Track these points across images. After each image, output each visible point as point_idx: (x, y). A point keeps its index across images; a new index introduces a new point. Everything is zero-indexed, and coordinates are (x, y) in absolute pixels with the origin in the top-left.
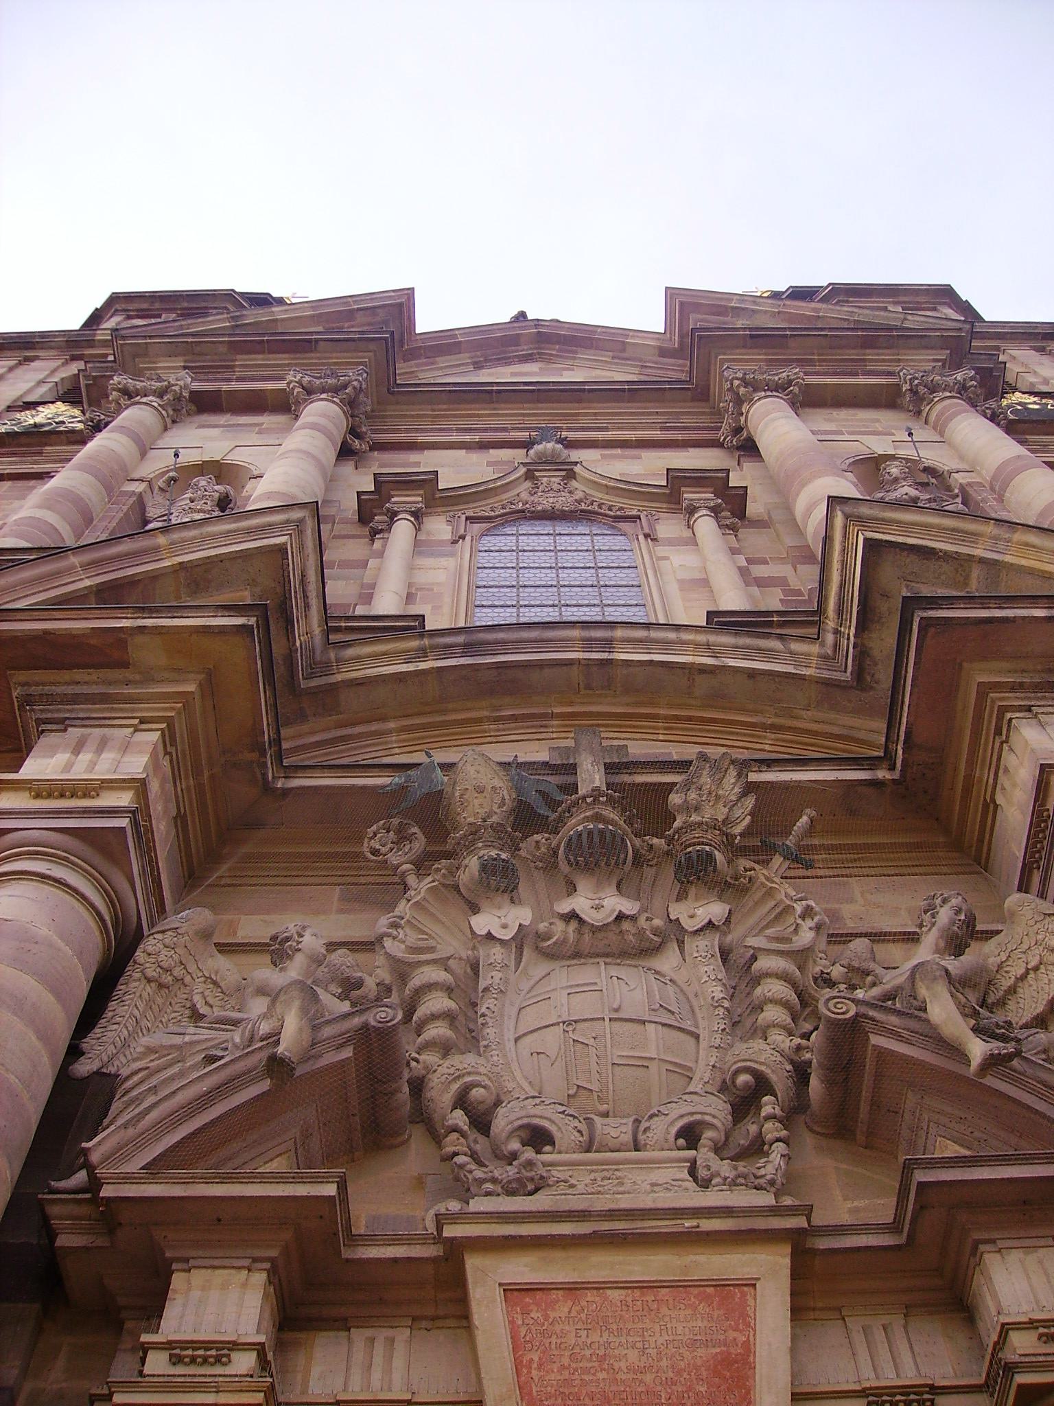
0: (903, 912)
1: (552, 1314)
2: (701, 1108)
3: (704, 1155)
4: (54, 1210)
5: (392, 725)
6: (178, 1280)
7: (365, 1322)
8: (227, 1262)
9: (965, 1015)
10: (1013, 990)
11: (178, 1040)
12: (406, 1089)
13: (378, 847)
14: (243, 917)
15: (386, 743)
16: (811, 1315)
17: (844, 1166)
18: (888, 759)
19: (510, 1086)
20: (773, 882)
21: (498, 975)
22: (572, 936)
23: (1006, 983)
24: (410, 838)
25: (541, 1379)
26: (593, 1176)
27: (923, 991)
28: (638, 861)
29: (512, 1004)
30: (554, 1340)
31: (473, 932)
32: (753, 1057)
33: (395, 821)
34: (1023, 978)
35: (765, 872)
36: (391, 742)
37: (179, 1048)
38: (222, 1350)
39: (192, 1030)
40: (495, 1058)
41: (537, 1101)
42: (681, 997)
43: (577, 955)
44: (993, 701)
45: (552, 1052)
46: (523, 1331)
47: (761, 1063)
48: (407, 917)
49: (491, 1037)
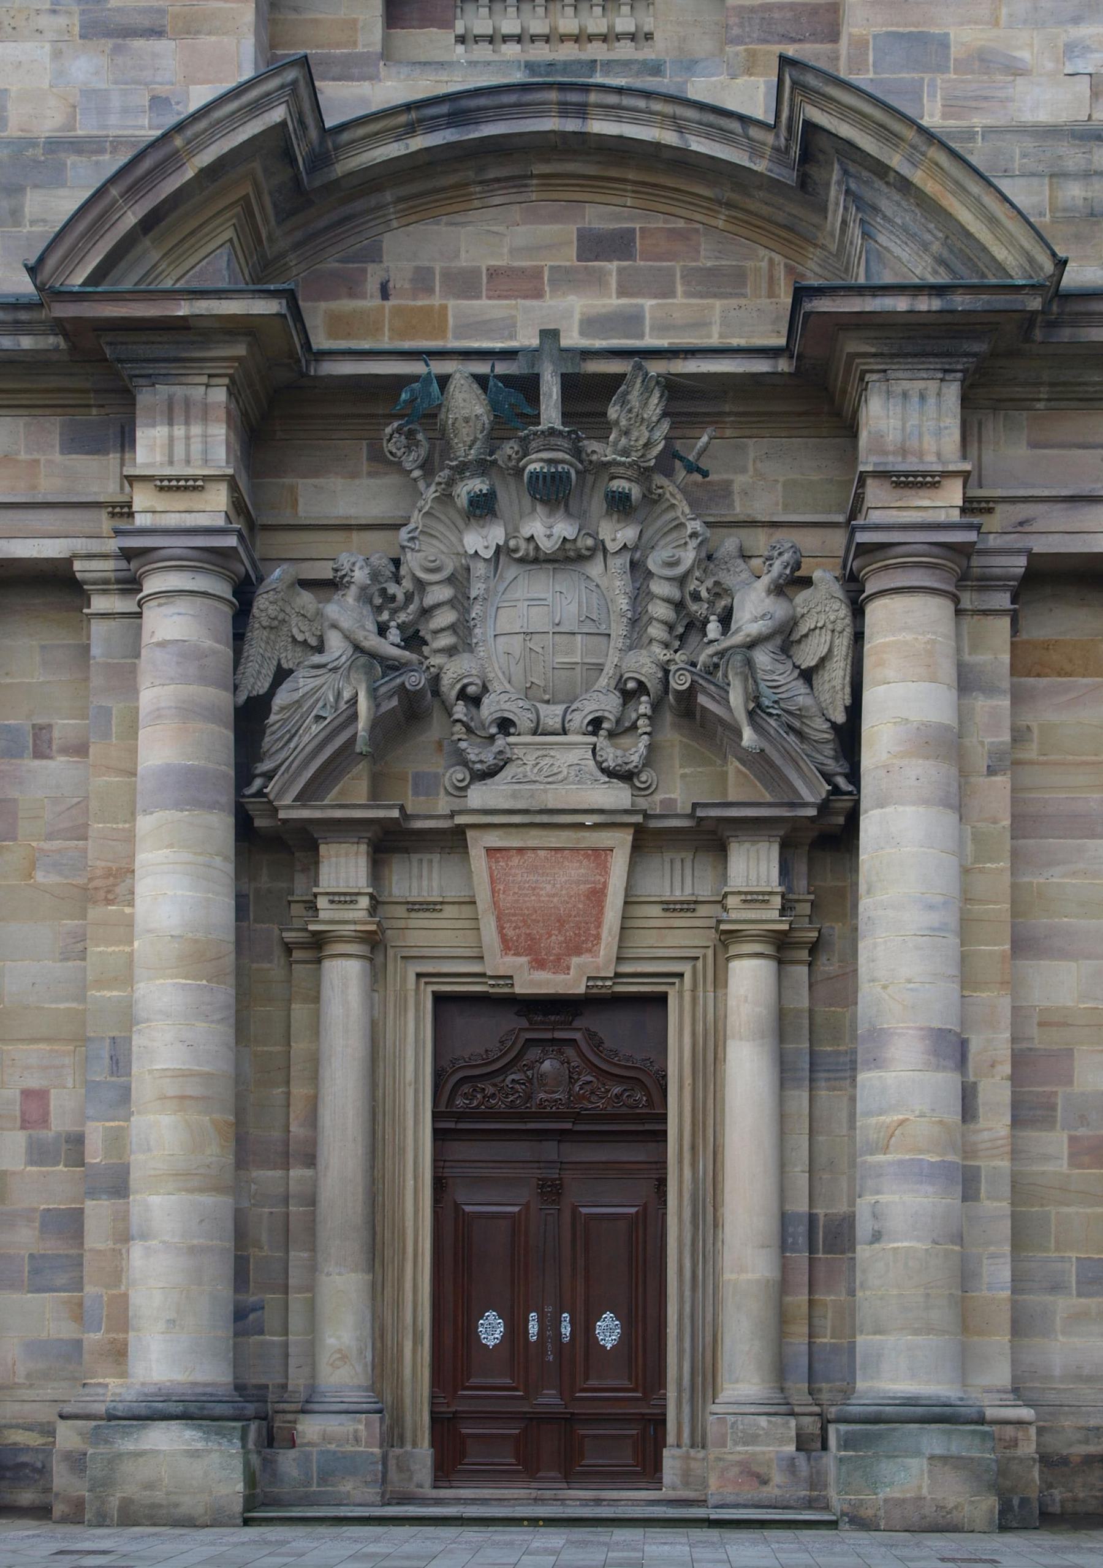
1: (510, 864)
5: (388, 196)
10: (806, 636)
14: (300, 481)
15: (384, 216)
20: (675, 498)
22: (532, 553)
36: (389, 214)
40: (482, 654)
43: (536, 561)
49: (479, 636)
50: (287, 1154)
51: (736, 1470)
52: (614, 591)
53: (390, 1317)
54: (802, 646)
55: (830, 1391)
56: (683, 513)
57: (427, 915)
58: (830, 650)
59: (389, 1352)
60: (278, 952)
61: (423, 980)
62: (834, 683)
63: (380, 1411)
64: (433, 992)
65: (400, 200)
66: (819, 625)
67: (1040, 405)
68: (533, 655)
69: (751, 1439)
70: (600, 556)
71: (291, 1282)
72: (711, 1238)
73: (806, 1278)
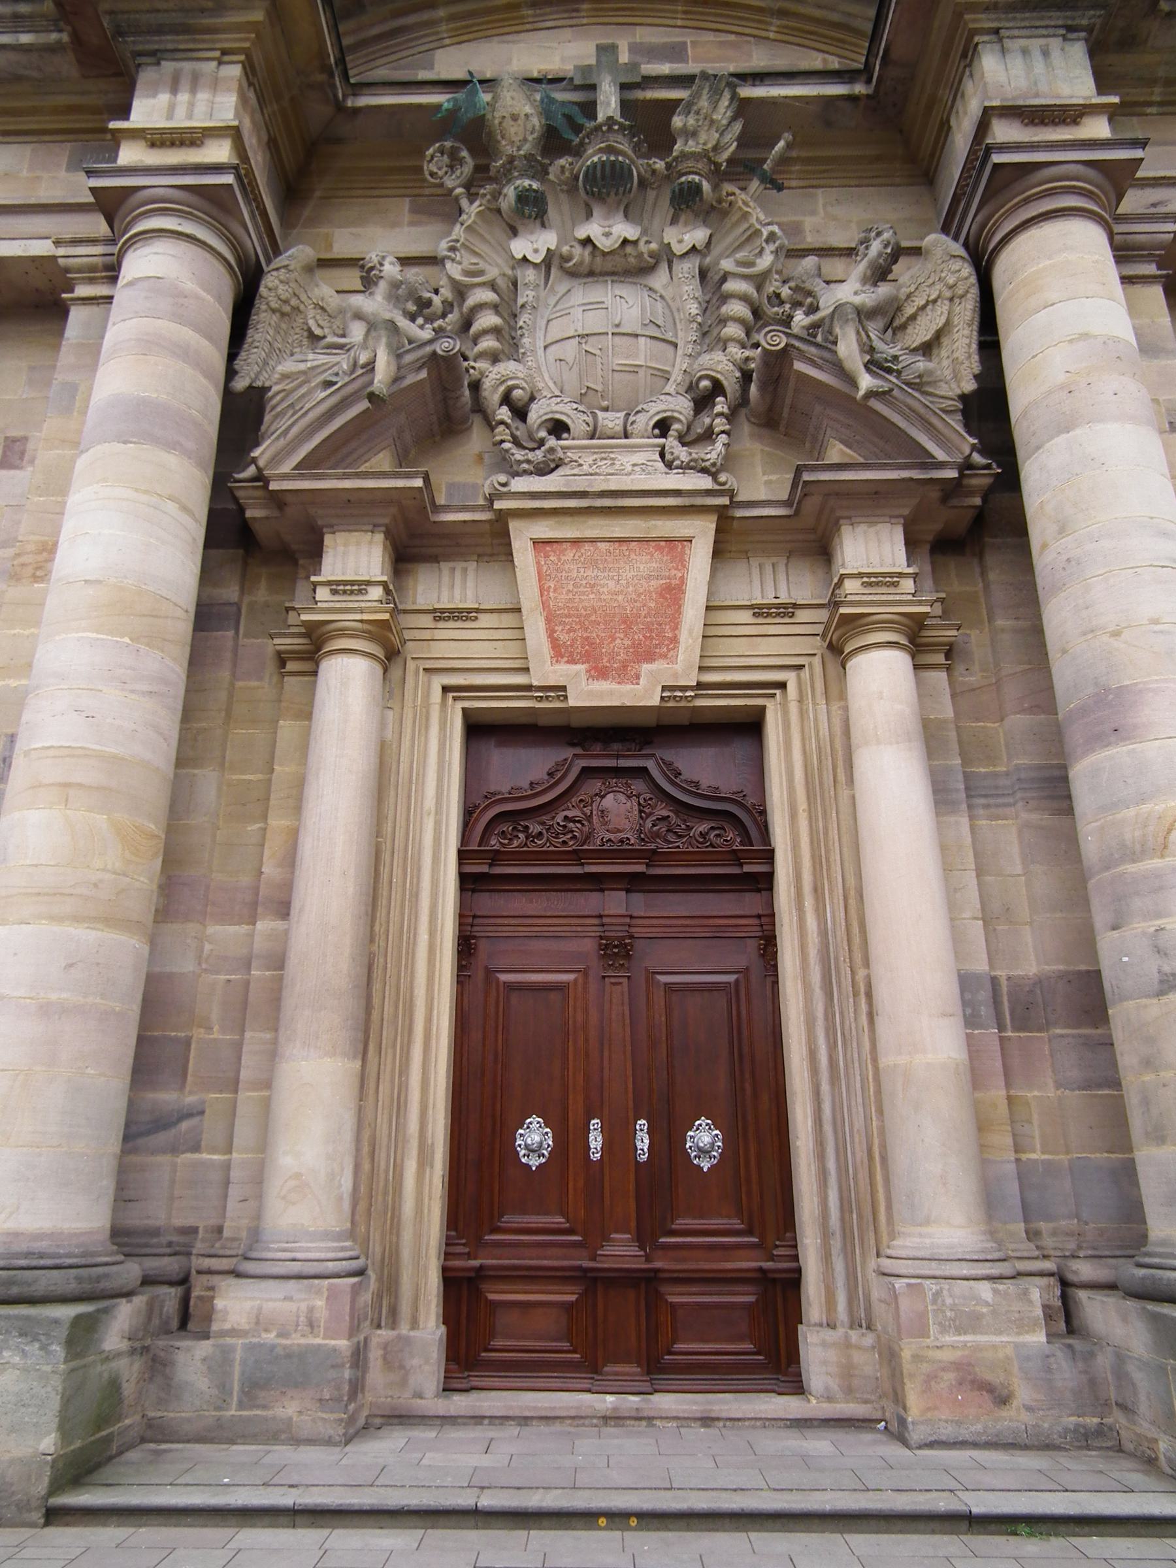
0: (853, 226)
1: (563, 558)
2: (672, 407)
3: (671, 442)
4: (239, 494)
5: (441, 13)
6: (328, 539)
7: (448, 558)
8: (358, 527)
9: (862, 351)
10: (913, 317)
11: (302, 366)
12: (467, 393)
13: (435, 170)
15: (437, 33)
16: (728, 555)
17: (767, 449)
18: (865, 73)
19: (540, 385)
20: (749, 206)
21: (531, 294)
22: (587, 258)
23: (909, 310)
24: (461, 162)
25: (556, 598)
26: (595, 456)
27: (837, 330)
28: (643, 183)
29: (542, 317)
30: (564, 574)
31: (513, 257)
32: (714, 367)
33: (448, 144)
34: (923, 308)
35: (743, 196)
37: (304, 373)
38: (360, 587)
39: (311, 356)
41: (559, 400)
42: (667, 312)
43: (591, 274)
44: (966, 24)
45: (570, 360)
46: (545, 569)
47: (718, 372)
48: (462, 240)
49: (527, 346)
50: (255, 904)
51: (950, 1377)
52: (681, 297)
53: (385, 1126)
54: (910, 330)
55: (1054, 1233)
56: (758, 219)
57: (459, 624)
58: (948, 323)
59: (382, 1176)
60: (271, 666)
61: (451, 695)
62: (955, 355)
63: (361, 1273)
64: (464, 709)
65: (452, 18)
66: (932, 297)
67: (1149, 110)
68: (590, 357)
69: (969, 1322)
70: (664, 266)
71: (244, 1075)
72: (852, 1010)
73: (998, 1064)
